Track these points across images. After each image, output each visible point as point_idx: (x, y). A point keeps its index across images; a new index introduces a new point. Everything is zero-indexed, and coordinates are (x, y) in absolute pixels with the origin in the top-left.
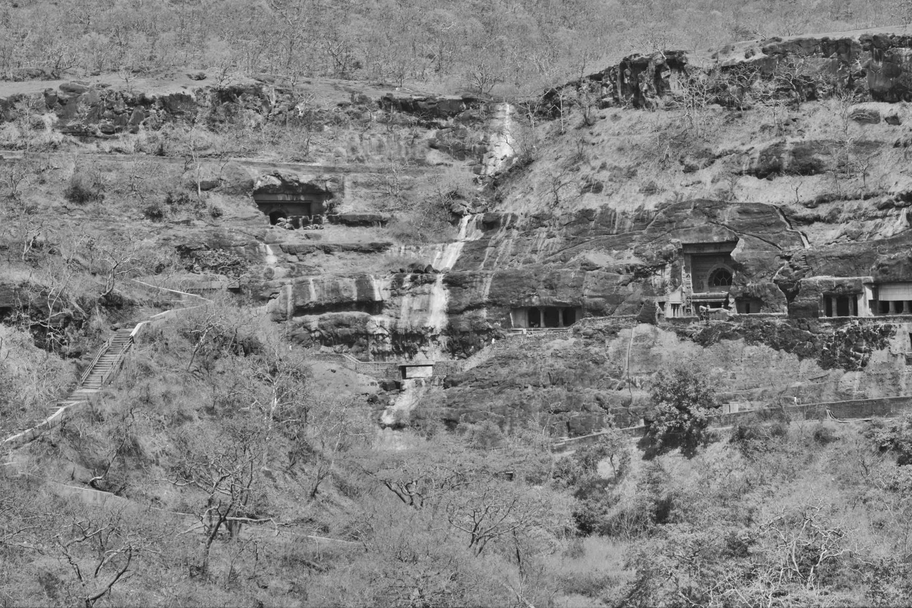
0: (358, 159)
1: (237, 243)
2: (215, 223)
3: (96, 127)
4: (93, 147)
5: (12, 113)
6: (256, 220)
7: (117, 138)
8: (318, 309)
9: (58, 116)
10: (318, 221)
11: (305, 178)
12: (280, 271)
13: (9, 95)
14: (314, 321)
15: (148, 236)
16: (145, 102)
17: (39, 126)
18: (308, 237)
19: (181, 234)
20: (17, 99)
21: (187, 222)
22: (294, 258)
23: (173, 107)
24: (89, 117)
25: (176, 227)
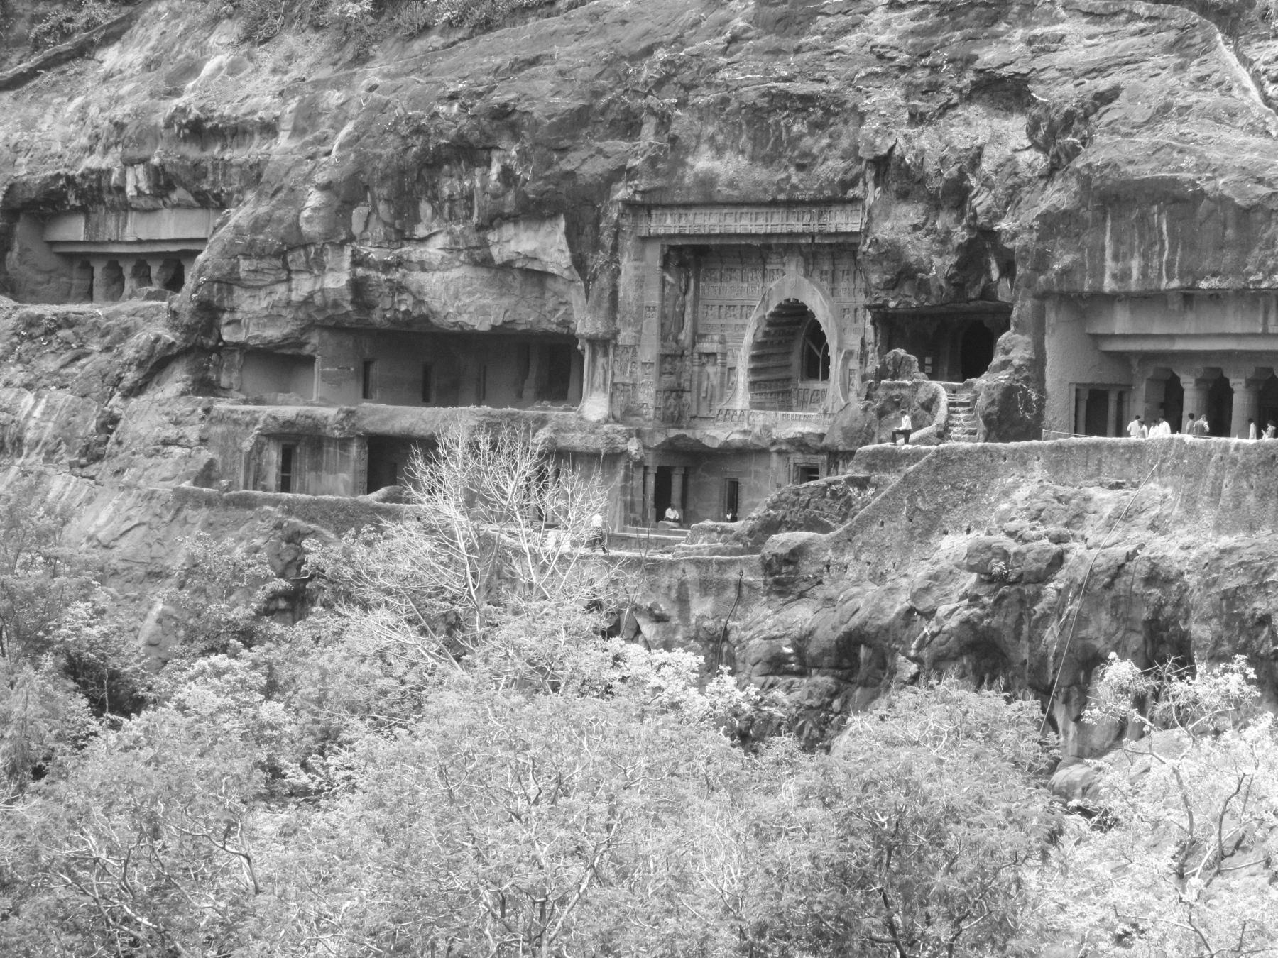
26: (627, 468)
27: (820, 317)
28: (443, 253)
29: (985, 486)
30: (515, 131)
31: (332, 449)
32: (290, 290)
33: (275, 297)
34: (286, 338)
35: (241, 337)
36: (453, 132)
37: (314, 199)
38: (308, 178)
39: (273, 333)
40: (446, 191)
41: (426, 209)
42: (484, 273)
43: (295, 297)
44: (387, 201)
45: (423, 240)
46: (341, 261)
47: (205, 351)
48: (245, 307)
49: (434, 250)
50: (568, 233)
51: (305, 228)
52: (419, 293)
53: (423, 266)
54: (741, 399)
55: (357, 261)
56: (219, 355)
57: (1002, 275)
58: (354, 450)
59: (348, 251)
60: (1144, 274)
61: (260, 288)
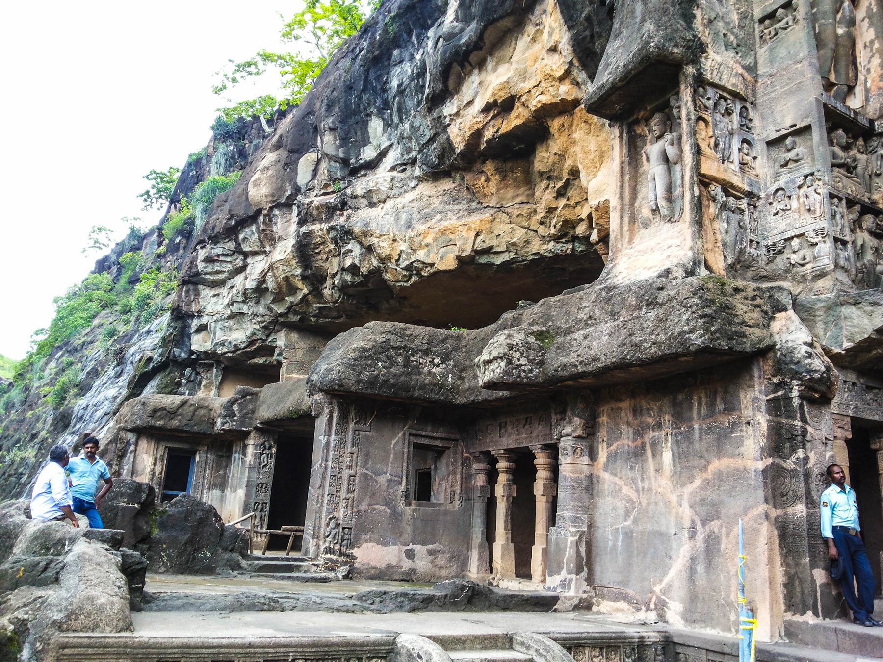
26: (778, 407)
28: (395, 173)
31: (237, 455)
32: (246, 278)
33: (234, 291)
34: (252, 343)
35: (208, 346)
39: (239, 336)
43: (250, 284)
45: (372, 165)
46: (289, 226)
47: (182, 365)
48: (209, 309)
52: (365, 234)
56: (194, 369)
61: (222, 283)
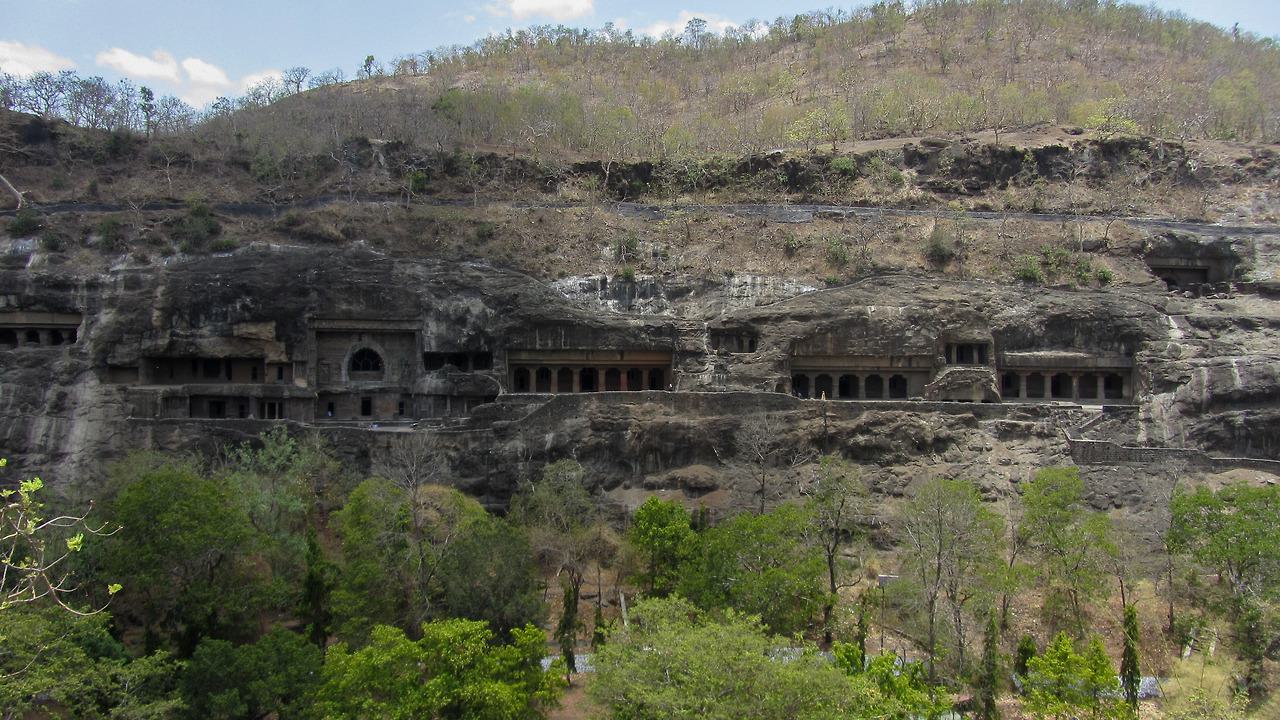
0: (1268, 218)
1: (1132, 313)
2: (1104, 289)
3: (959, 183)
4: (956, 203)
5: (866, 170)
6: (1153, 286)
7: (984, 194)
8: (1245, 399)
9: (917, 171)
10: (1226, 289)
11: (1205, 239)
12: (1189, 350)
13: (866, 151)
14: (1239, 416)
15: (1020, 302)
16: (1015, 156)
17: (896, 182)
18: (1220, 308)
19: (1060, 301)
20: (872, 155)
21: (1066, 288)
22: (1206, 334)
23: (1049, 162)
24: (953, 171)
25: (1054, 293)
27: (379, 352)
29: (578, 406)
30: (248, 293)
35: (115, 362)
36: (220, 292)
37: (156, 313)
38: (151, 306)
39: (127, 360)
40: (214, 312)
41: (202, 317)
42: (224, 339)
43: (143, 347)
44: (189, 315)
49: (205, 331)
50: (276, 328)
51: (155, 324)
53: (201, 336)
54: (344, 378)
55: (173, 334)
57: (485, 343)
58: (188, 401)
59: (169, 331)
60: (554, 344)
